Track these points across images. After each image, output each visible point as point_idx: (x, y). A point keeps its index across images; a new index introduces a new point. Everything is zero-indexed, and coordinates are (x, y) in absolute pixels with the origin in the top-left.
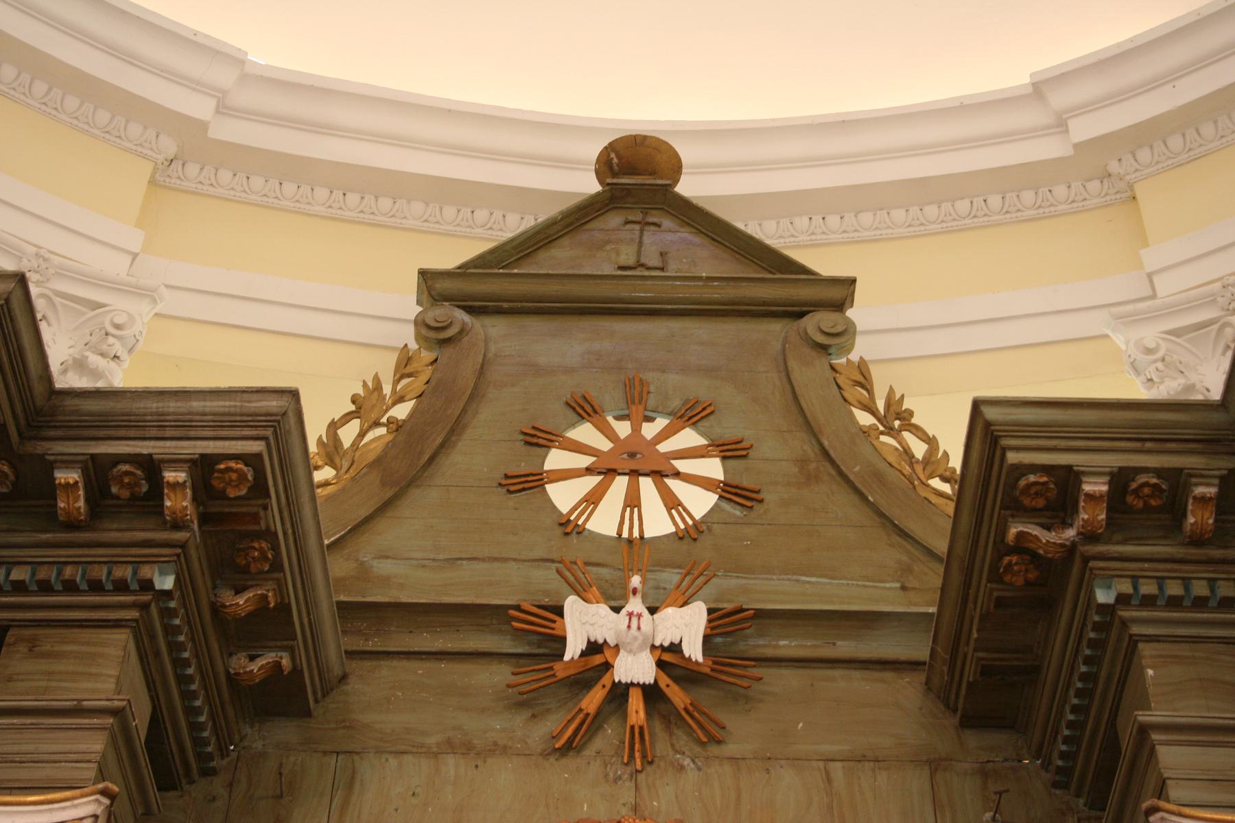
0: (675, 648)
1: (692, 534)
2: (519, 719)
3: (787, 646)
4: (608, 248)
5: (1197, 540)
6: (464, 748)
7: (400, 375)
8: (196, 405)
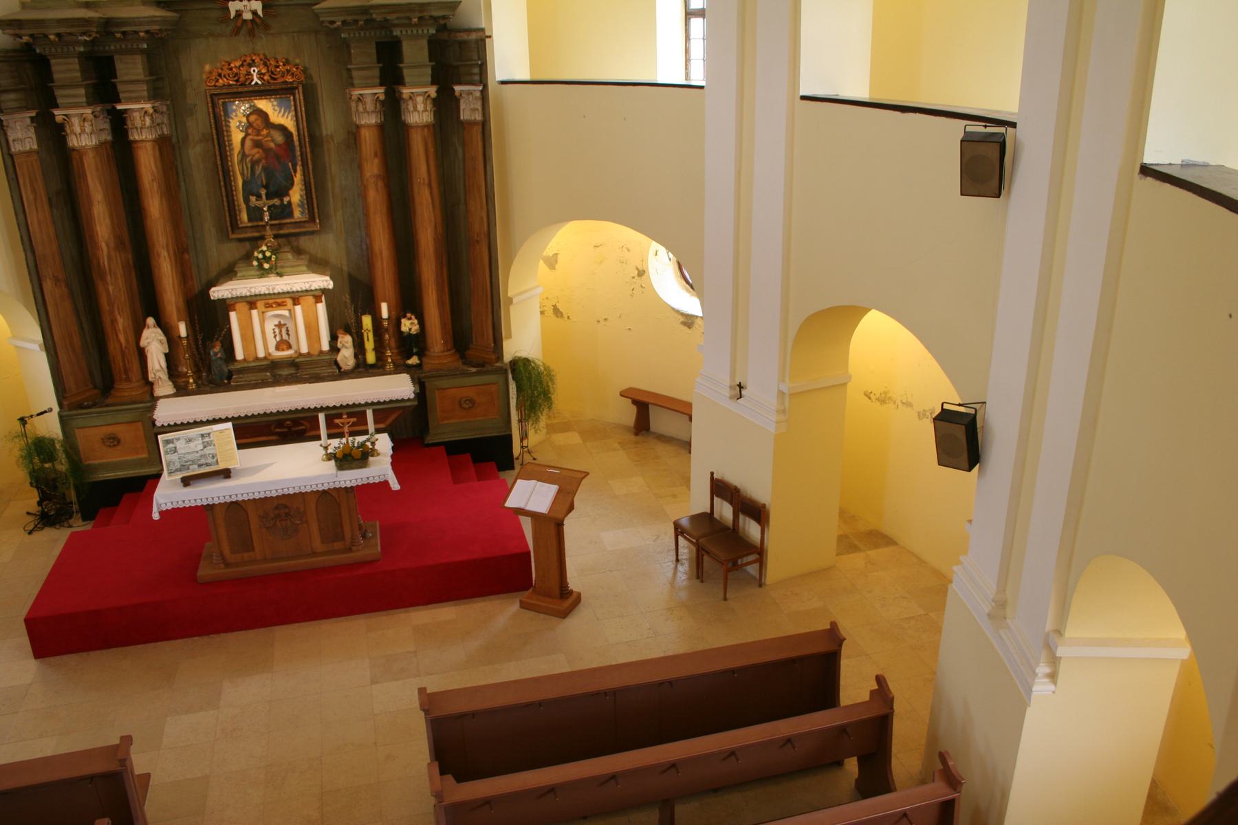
0: (256, 10)
8: (141, 20)
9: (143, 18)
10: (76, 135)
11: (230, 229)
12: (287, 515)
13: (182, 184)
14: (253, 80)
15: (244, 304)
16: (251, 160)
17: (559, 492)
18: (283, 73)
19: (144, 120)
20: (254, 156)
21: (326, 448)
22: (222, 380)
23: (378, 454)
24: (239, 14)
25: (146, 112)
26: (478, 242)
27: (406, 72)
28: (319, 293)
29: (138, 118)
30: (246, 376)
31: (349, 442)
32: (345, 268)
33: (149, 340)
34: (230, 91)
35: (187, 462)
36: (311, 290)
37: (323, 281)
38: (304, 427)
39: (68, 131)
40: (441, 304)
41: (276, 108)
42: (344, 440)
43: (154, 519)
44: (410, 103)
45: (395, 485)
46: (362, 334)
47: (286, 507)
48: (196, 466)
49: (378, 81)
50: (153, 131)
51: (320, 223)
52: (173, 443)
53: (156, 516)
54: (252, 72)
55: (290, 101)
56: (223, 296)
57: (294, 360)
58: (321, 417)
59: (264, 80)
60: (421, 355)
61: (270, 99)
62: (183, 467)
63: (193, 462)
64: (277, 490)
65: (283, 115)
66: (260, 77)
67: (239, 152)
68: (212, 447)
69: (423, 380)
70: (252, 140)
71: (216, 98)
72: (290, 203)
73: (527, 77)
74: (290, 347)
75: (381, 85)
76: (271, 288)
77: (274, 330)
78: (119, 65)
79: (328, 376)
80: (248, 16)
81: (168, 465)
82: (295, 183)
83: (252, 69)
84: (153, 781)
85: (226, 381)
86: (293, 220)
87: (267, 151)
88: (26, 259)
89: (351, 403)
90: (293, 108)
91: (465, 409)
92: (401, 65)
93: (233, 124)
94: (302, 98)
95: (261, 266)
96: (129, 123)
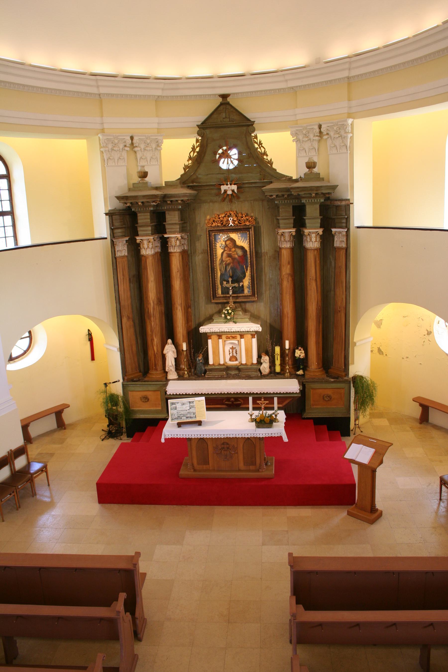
0: (234, 190)
1: (235, 168)
2: (218, 197)
3: (246, 186)
4: (221, 114)
5: (286, 197)
6: (212, 201)
7: (196, 143)
8: (180, 195)
9: (181, 194)
10: (145, 249)
11: (212, 297)
12: (228, 448)
13: (191, 274)
14: (229, 224)
15: (216, 336)
16: (226, 263)
17: (375, 453)
18: (245, 220)
19: (176, 243)
20: (227, 261)
21: (251, 415)
22: (201, 374)
23: (278, 422)
24: (225, 191)
25: (177, 239)
26: (339, 311)
27: (307, 221)
28: (254, 333)
29: (174, 241)
30: (213, 373)
31: (264, 413)
32: (268, 321)
33: (168, 351)
34: (218, 229)
35: (181, 415)
36: (250, 331)
37: (257, 327)
38: (240, 402)
39: (142, 247)
40: (317, 343)
41: (240, 238)
42: (261, 412)
43: (162, 442)
44: (308, 237)
45: (286, 439)
46: (275, 356)
47: (227, 444)
48: (185, 418)
49: (292, 225)
50: (180, 248)
51: (257, 297)
52: (175, 404)
53: (163, 441)
54: (230, 220)
55: (247, 234)
56: (206, 331)
57: (238, 367)
58: (251, 399)
59: (235, 224)
60: (304, 369)
61: (237, 233)
62: (179, 418)
63: (184, 415)
64: (224, 435)
65: (243, 242)
66: (233, 222)
67: (220, 259)
68: (194, 409)
69: (304, 383)
70: (227, 253)
71: (211, 232)
72: (243, 285)
73: (371, 225)
74: (236, 360)
75: (294, 227)
76: (230, 329)
77: (229, 350)
78: (167, 216)
79: (255, 377)
80: (230, 192)
81: (172, 415)
82: (246, 276)
83: (230, 218)
84: (147, 577)
85: (203, 375)
86: (244, 295)
87: (233, 259)
88: (116, 307)
89: (265, 392)
90: (248, 238)
91: (326, 400)
92: (305, 218)
93: (218, 245)
94: (253, 233)
95: (226, 317)
96: (169, 243)
